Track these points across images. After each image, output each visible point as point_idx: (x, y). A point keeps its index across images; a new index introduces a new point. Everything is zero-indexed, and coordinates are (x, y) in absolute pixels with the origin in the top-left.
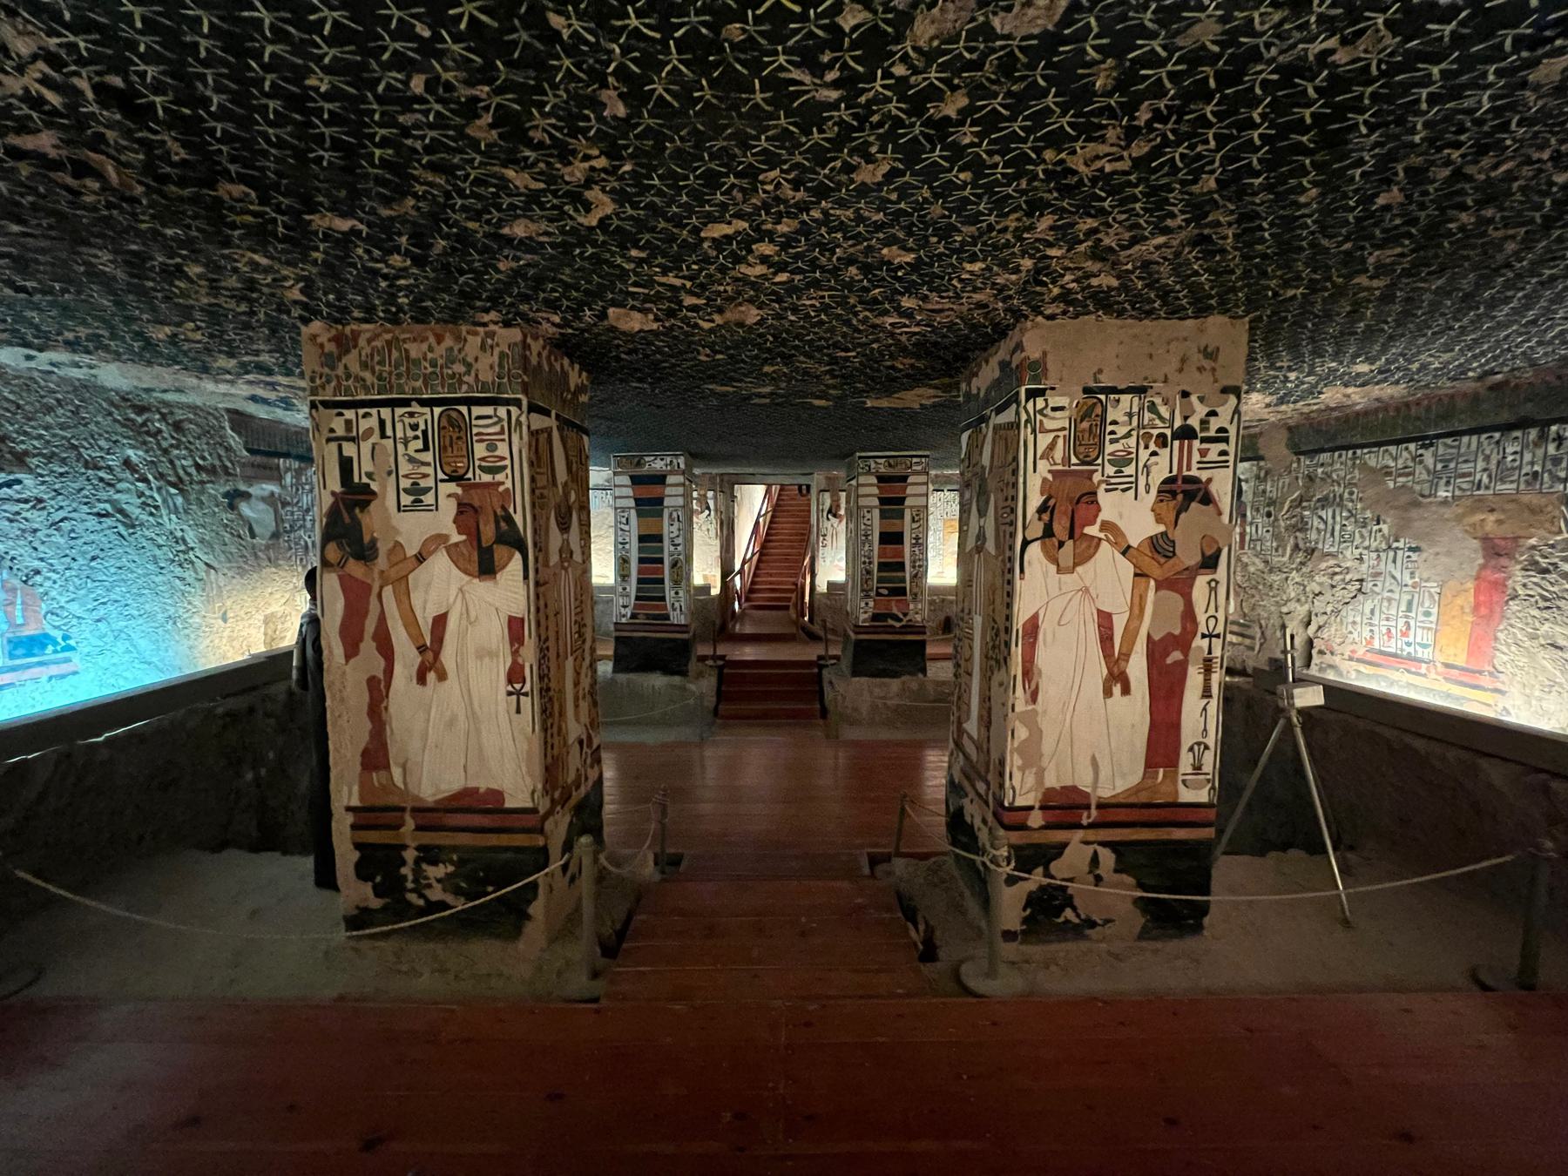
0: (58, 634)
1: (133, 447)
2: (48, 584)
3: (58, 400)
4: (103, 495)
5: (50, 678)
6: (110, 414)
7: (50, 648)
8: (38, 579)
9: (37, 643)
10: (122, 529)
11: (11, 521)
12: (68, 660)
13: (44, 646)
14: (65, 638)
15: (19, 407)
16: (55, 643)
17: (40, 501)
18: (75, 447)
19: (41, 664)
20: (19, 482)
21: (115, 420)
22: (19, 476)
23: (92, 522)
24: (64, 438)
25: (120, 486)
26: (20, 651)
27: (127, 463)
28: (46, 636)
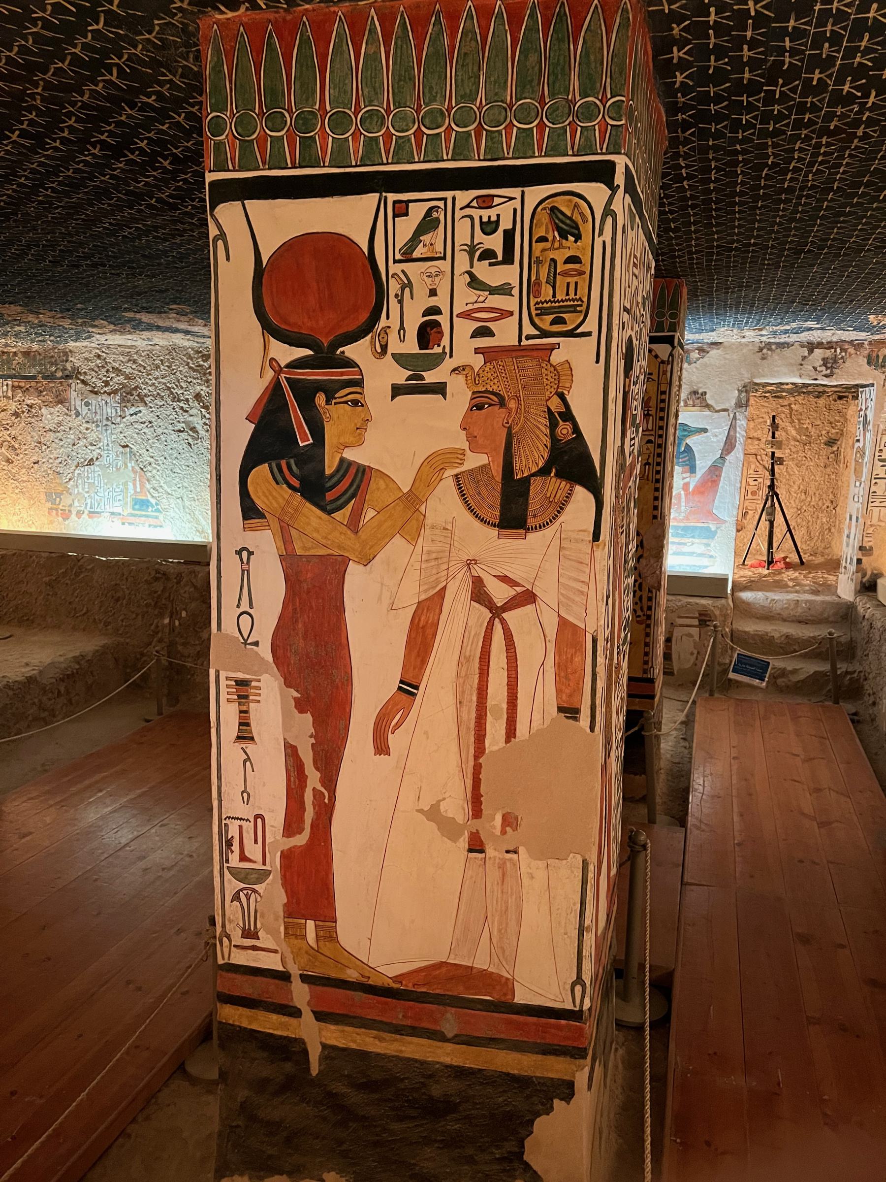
0: (153, 501)
1: (200, 385)
2: (154, 471)
3: (161, 360)
4: (181, 419)
5: (150, 526)
6: (188, 364)
7: (150, 509)
8: (149, 468)
9: (143, 504)
10: (190, 440)
11: (138, 434)
12: (157, 518)
13: (148, 507)
14: (157, 504)
15: (145, 368)
16: (153, 507)
17: (150, 422)
18: (169, 388)
19: (147, 516)
20: (140, 411)
21: (190, 368)
22: (141, 408)
23: (174, 436)
24: (164, 384)
25: (191, 412)
26: (137, 507)
27: (198, 397)
28: (148, 501)
